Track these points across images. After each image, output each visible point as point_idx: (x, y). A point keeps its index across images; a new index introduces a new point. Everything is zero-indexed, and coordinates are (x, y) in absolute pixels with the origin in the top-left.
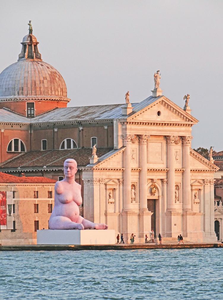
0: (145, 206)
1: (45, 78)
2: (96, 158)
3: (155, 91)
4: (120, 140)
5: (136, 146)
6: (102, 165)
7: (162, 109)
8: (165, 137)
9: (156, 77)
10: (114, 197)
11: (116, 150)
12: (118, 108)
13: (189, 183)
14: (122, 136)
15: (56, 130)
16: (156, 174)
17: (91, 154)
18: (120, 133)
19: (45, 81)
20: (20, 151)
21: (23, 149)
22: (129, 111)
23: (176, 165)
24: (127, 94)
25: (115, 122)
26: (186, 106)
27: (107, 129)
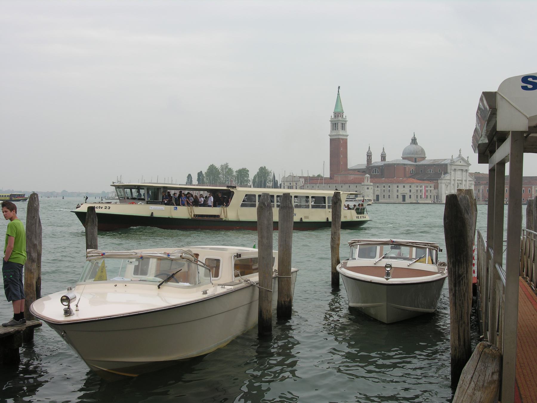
1: (420, 150)
5: (454, 172)
8: (462, 169)
9: (460, 150)
11: (448, 173)
12: (446, 160)
13: (468, 184)
14: (451, 169)
15: (426, 167)
17: (442, 175)
19: (420, 151)
21: (414, 173)
22: (453, 161)
24: (452, 156)
25: (448, 165)
26: (468, 160)
27: (444, 167)
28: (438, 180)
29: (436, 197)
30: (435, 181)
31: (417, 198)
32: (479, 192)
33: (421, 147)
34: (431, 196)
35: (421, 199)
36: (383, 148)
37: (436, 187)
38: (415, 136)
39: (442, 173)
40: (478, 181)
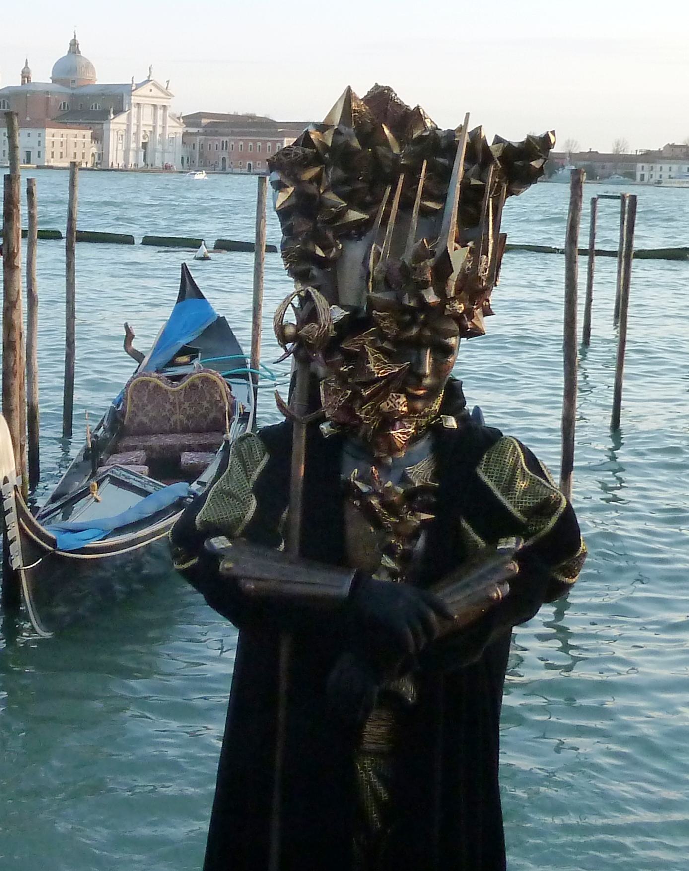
0: (141, 145)
2: (112, 116)
3: (149, 77)
4: (127, 106)
6: (116, 120)
7: (153, 88)
10: (122, 140)
11: (126, 111)
13: (167, 133)
16: (147, 127)
18: (127, 102)
20: (66, 109)
22: (133, 88)
23: (160, 122)
24: (133, 78)
25: (124, 95)
26: (167, 88)
28: (103, 123)
29: (99, 157)
30: (99, 127)
31: (53, 157)
32: (194, 149)
33: (86, 59)
34: (84, 154)
35: (62, 159)
36: (27, 60)
37: (98, 138)
38: (77, 39)
39: (109, 111)
40: (216, 129)
